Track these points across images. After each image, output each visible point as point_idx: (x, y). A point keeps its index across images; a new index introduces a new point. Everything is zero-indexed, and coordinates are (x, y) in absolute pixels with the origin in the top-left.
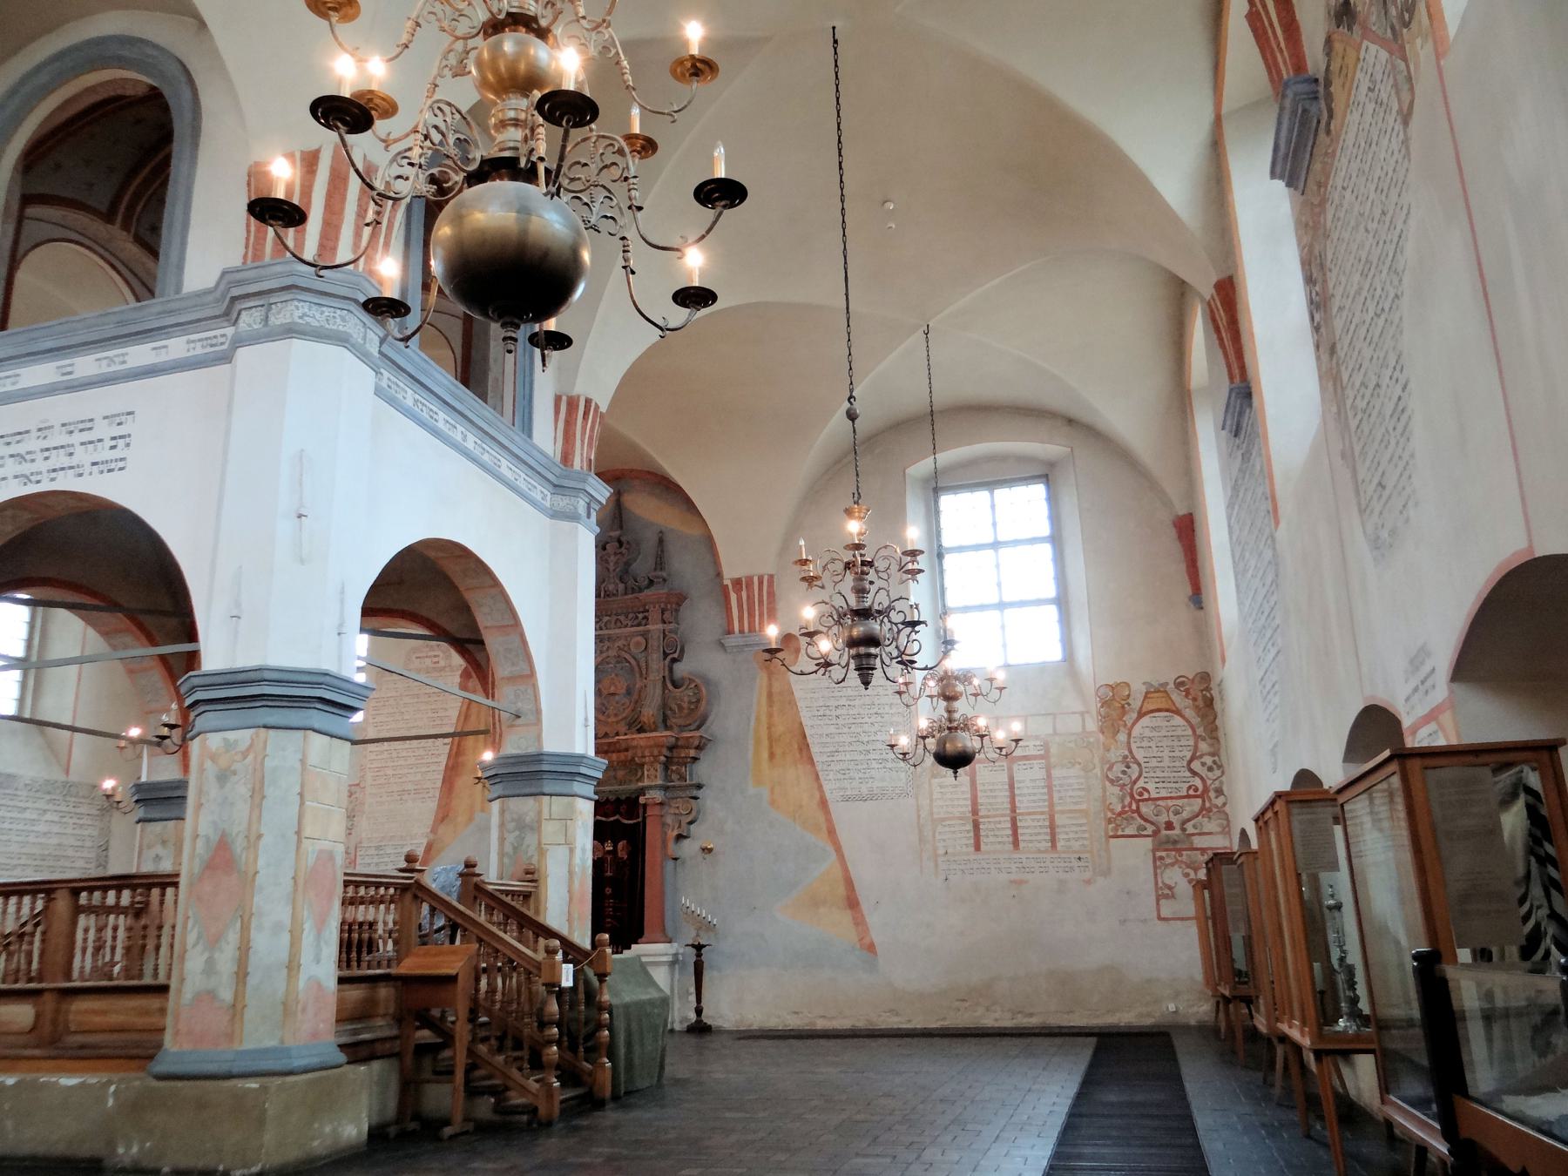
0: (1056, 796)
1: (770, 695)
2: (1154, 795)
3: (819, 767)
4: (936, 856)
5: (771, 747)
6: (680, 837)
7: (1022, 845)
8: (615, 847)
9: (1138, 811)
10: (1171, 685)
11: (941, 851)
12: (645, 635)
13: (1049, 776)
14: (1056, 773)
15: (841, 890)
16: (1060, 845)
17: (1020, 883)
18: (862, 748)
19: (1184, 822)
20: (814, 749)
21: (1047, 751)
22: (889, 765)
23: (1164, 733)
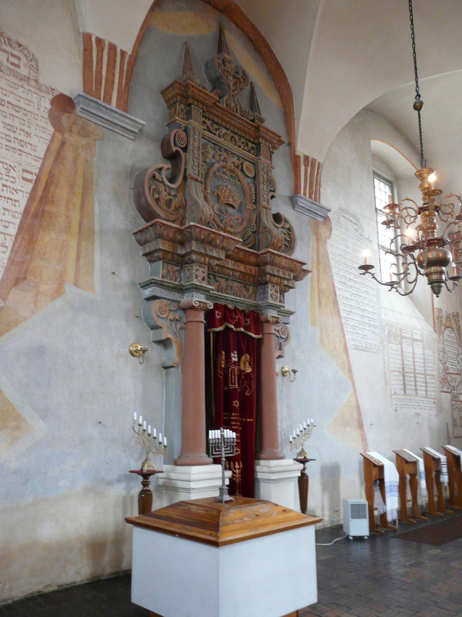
0: (427, 365)
1: (318, 255)
2: (451, 372)
3: (343, 321)
4: (391, 394)
5: (319, 296)
6: (280, 357)
7: (418, 392)
8: (239, 358)
9: (446, 379)
10: (451, 316)
11: (393, 392)
12: (255, 164)
13: (424, 352)
14: (426, 351)
15: (355, 415)
16: (429, 393)
17: (418, 414)
18: (361, 313)
19: (458, 386)
20: (341, 307)
21: (422, 337)
22: (373, 329)
23: (451, 340)
